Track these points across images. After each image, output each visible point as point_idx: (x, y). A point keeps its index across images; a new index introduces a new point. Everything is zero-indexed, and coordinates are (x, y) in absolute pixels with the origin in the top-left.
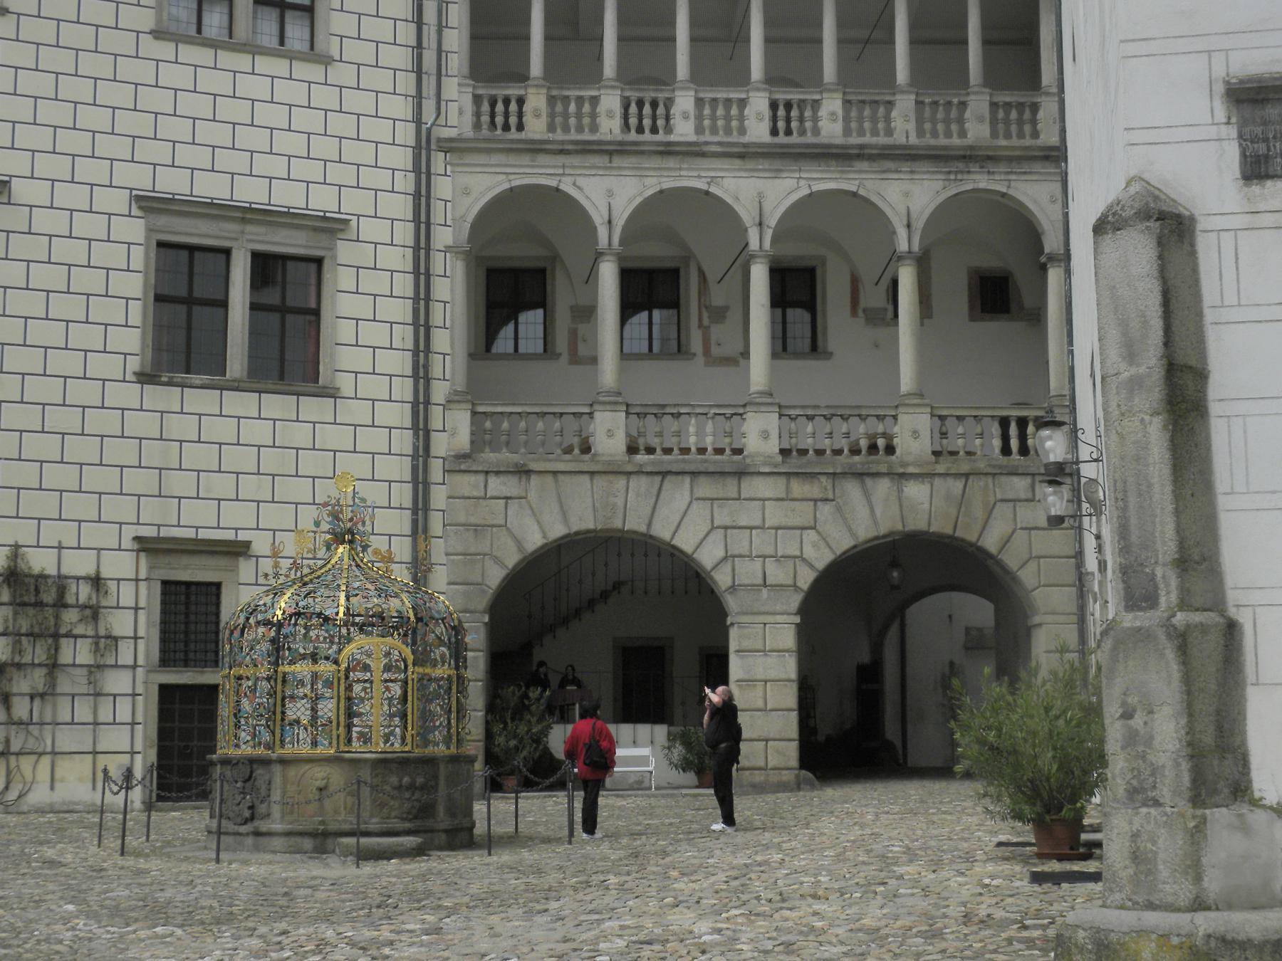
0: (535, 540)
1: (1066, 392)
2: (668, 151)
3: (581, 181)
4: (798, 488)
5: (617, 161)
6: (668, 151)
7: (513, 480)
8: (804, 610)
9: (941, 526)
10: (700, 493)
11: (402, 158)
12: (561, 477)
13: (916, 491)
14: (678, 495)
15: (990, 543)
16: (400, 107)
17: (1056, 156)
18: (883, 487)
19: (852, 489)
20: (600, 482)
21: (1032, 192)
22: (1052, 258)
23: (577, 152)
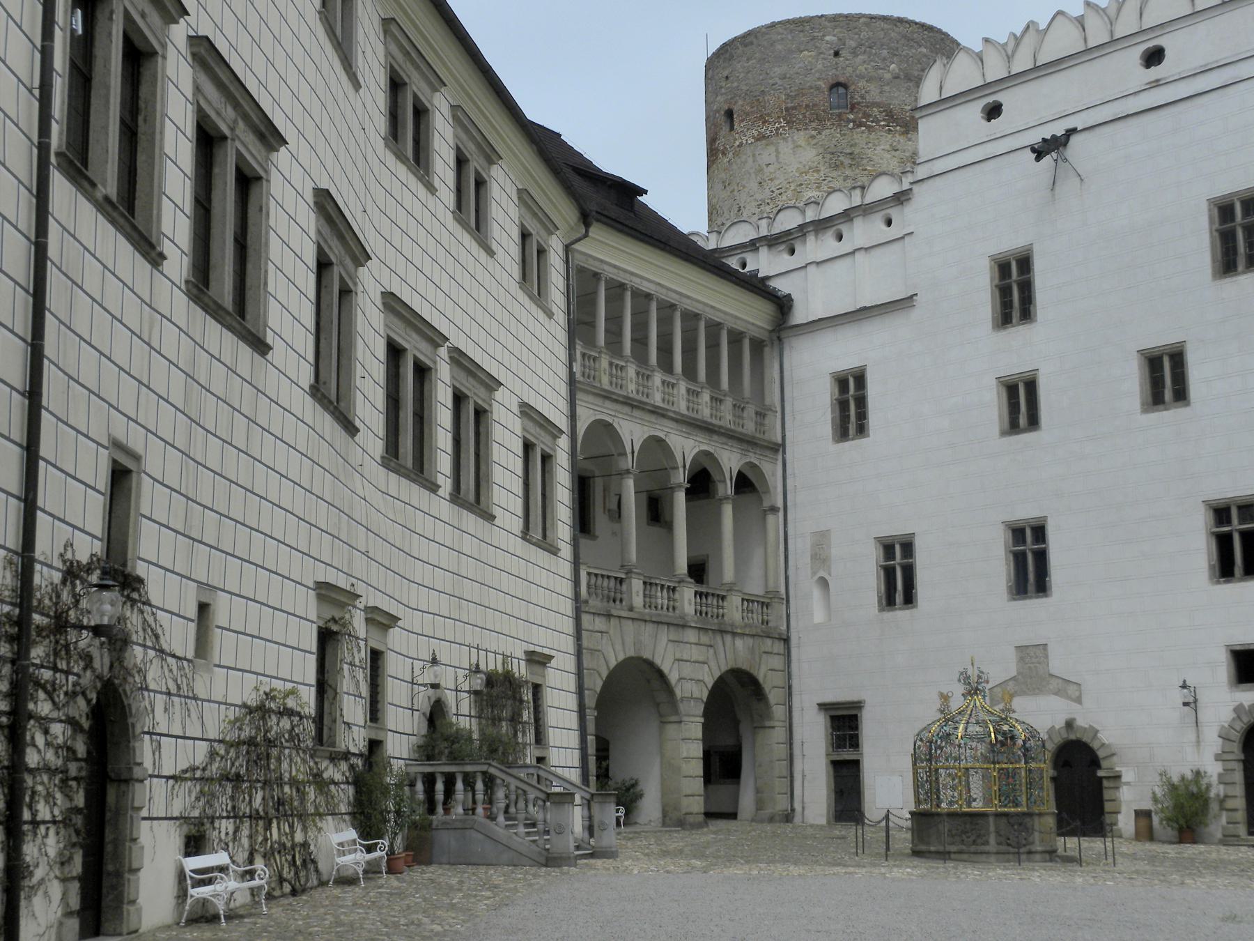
0: (613, 663)
1: (783, 590)
2: (657, 412)
3: (622, 422)
4: (705, 639)
5: (637, 413)
6: (657, 412)
7: (603, 619)
8: (705, 715)
9: (744, 667)
10: (671, 638)
11: (563, 389)
12: (623, 621)
13: (739, 643)
14: (664, 635)
15: (761, 680)
16: (563, 354)
17: (777, 448)
18: (728, 638)
19: (719, 638)
20: (637, 623)
21: (771, 470)
22: (774, 509)
23: (622, 403)
